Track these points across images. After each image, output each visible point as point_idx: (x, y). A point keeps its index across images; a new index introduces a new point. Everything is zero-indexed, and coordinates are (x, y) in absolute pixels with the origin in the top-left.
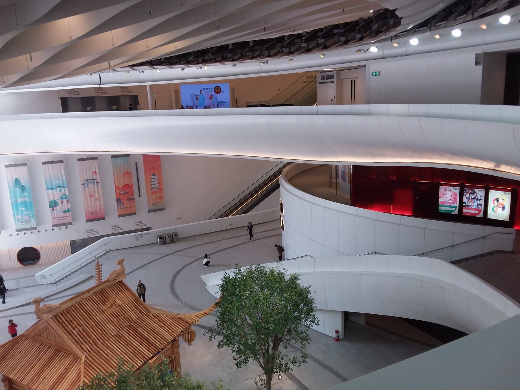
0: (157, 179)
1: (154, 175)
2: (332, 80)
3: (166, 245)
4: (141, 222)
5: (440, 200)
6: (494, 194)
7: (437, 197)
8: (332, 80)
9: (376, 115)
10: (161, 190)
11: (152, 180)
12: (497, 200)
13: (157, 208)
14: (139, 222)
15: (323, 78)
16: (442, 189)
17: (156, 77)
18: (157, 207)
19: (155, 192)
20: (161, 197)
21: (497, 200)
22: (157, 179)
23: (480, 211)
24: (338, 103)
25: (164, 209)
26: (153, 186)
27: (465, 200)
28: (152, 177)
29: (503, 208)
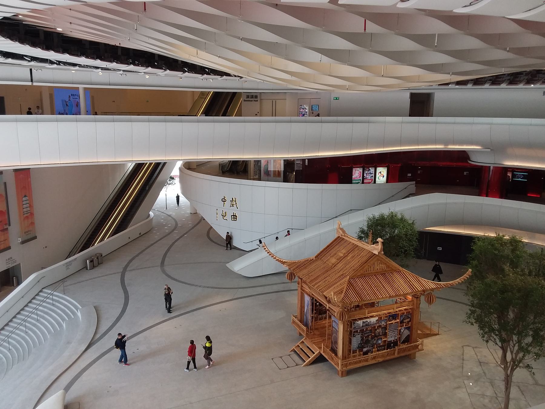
0: (28, 202)
1: (25, 196)
2: (256, 99)
3: (96, 269)
4: (11, 258)
5: (353, 177)
6: (379, 169)
7: (351, 175)
8: (256, 99)
9: (373, 123)
10: (32, 214)
11: (24, 203)
12: (380, 172)
13: (29, 237)
14: (9, 259)
15: (248, 97)
16: (354, 170)
17: (112, 81)
18: (29, 237)
19: (27, 217)
20: (33, 223)
21: (380, 172)
22: (28, 202)
23: (372, 180)
24: (261, 116)
25: (35, 238)
26: (25, 210)
27: (365, 175)
28: (24, 199)
29: (383, 176)
